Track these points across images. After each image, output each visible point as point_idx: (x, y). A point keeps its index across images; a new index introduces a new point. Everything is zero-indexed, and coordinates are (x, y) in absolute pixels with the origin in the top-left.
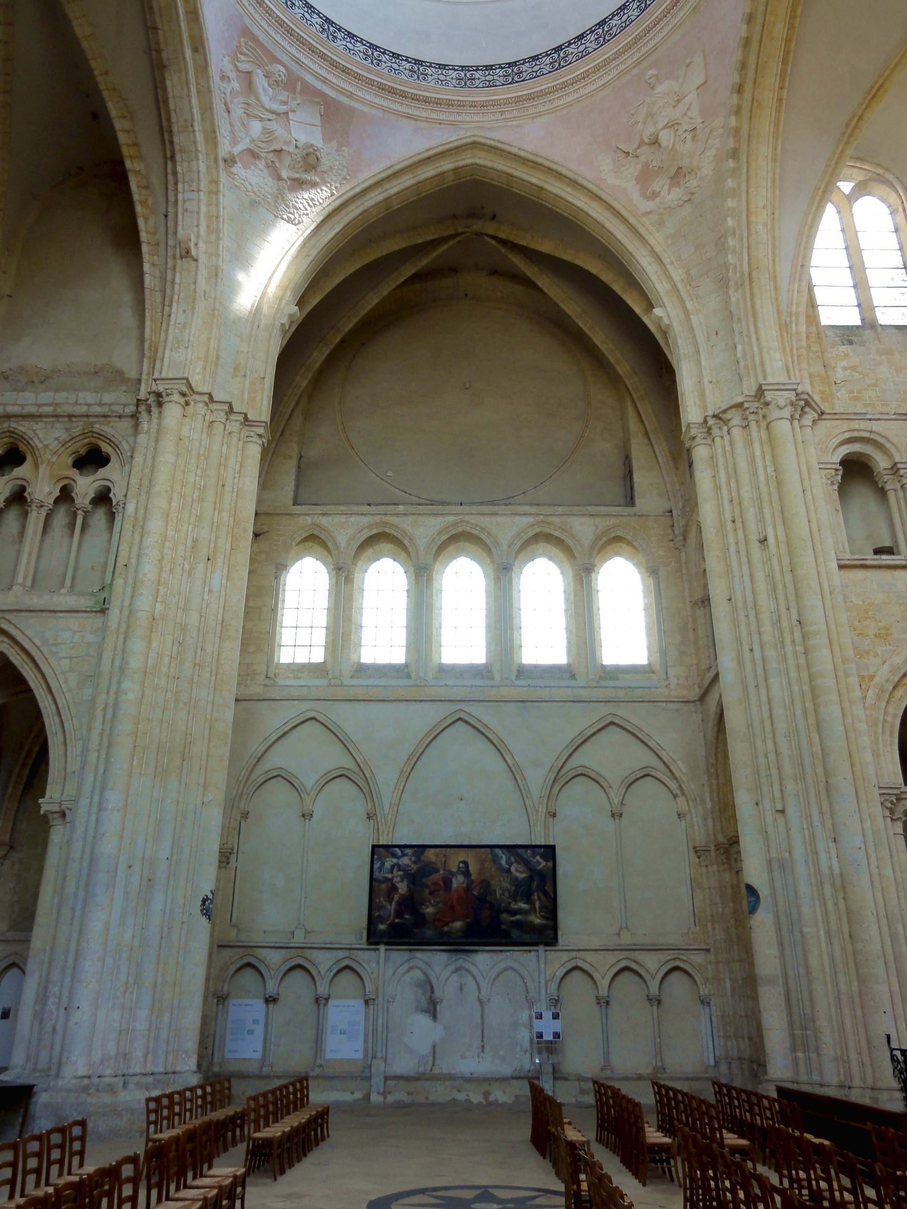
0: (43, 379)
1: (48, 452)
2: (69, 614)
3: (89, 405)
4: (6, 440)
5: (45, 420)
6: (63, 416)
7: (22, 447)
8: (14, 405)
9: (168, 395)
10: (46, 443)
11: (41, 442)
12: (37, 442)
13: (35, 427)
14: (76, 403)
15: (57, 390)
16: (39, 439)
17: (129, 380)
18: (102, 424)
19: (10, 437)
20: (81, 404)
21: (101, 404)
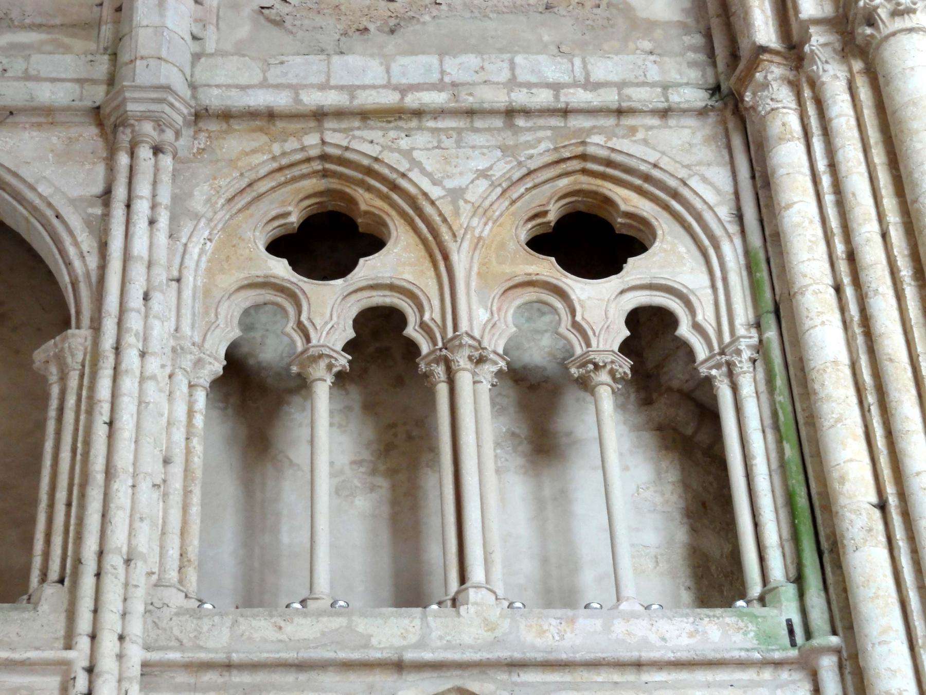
0: (392, 22)
1: (466, 210)
2: (683, 676)
3: (556, 87)
4: (313, 184)
5: (431, 124)
6: (492, 113)
7: (366, 201)
8: (324, 87)
9: (897, 13)
10: (450, 184)
11: (435, 183)
12: (425, 184)
13: (404, 143)
14: (513, 83)
15: (442, 54)
16: (429, 175)
17: (651, 25)
18: (610, 135)
19: (325, 174)
20: (529, 85)
21: (589, 85)
